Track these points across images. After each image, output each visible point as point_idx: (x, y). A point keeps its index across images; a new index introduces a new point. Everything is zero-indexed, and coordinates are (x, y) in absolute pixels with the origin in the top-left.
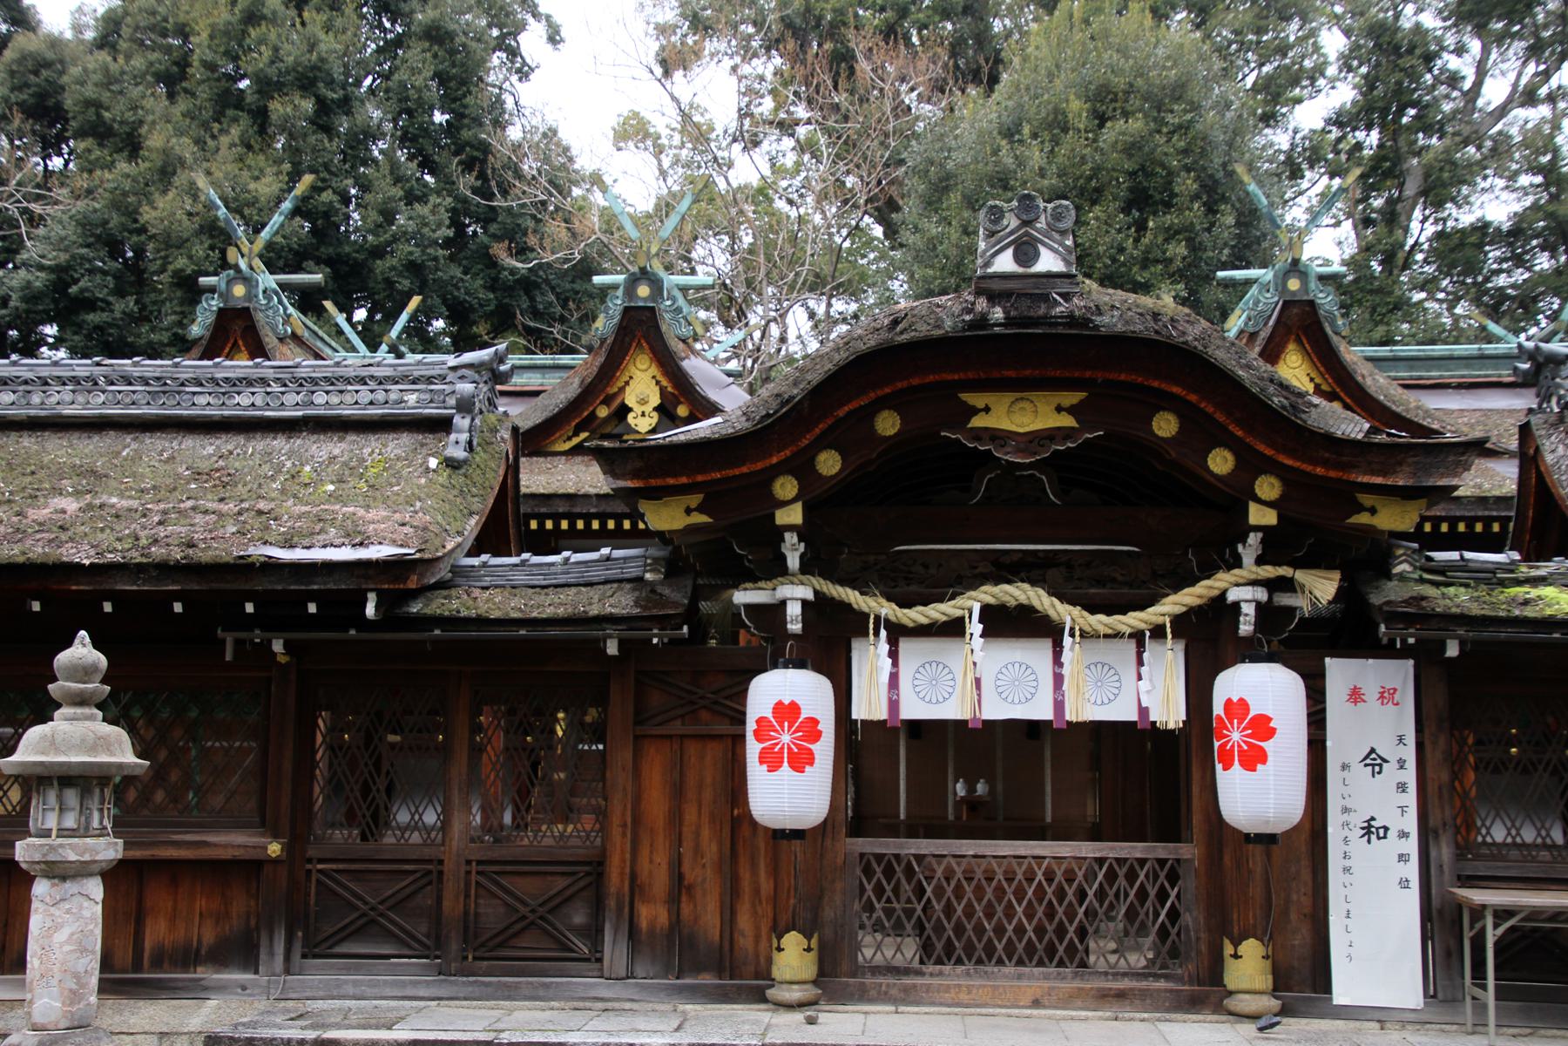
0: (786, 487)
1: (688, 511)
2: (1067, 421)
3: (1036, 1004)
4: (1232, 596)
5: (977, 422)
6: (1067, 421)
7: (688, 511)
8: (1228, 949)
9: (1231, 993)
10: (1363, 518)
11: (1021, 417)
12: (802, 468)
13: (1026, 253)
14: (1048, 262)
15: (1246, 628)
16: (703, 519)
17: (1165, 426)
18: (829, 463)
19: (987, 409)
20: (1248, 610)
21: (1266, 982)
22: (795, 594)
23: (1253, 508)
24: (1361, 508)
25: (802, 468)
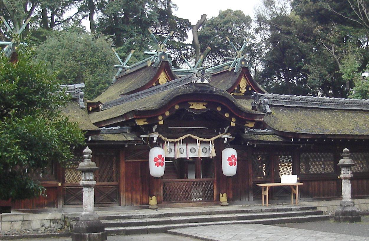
0: (160, 118)
1: (144, 122)
2: (205, 108)
3: (192, 206)
4: (223, 137)
5: (191, 107)
6: (205, 108)
7: (144, 122)
8: (221, 195)
9: (221, 202)
10: (247, 125)
11: (199, 107)
12: (163, 115)
13: (202, 80)
14: (206, 81)
15: (225, 142)
16: (146, 123)
17: (219, 109)
18: (167, 114)
19: (192, 105)
20: (226, 139)
21: (226, 200)
22: (155, 136)
23: (231, 122)
24: (246, 123)
25: (163, 115)
